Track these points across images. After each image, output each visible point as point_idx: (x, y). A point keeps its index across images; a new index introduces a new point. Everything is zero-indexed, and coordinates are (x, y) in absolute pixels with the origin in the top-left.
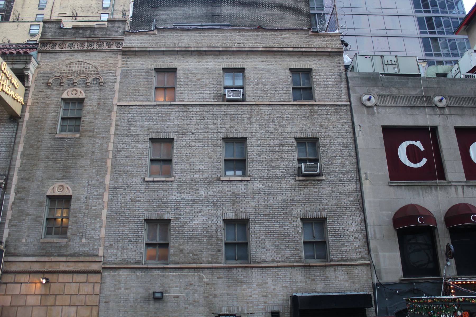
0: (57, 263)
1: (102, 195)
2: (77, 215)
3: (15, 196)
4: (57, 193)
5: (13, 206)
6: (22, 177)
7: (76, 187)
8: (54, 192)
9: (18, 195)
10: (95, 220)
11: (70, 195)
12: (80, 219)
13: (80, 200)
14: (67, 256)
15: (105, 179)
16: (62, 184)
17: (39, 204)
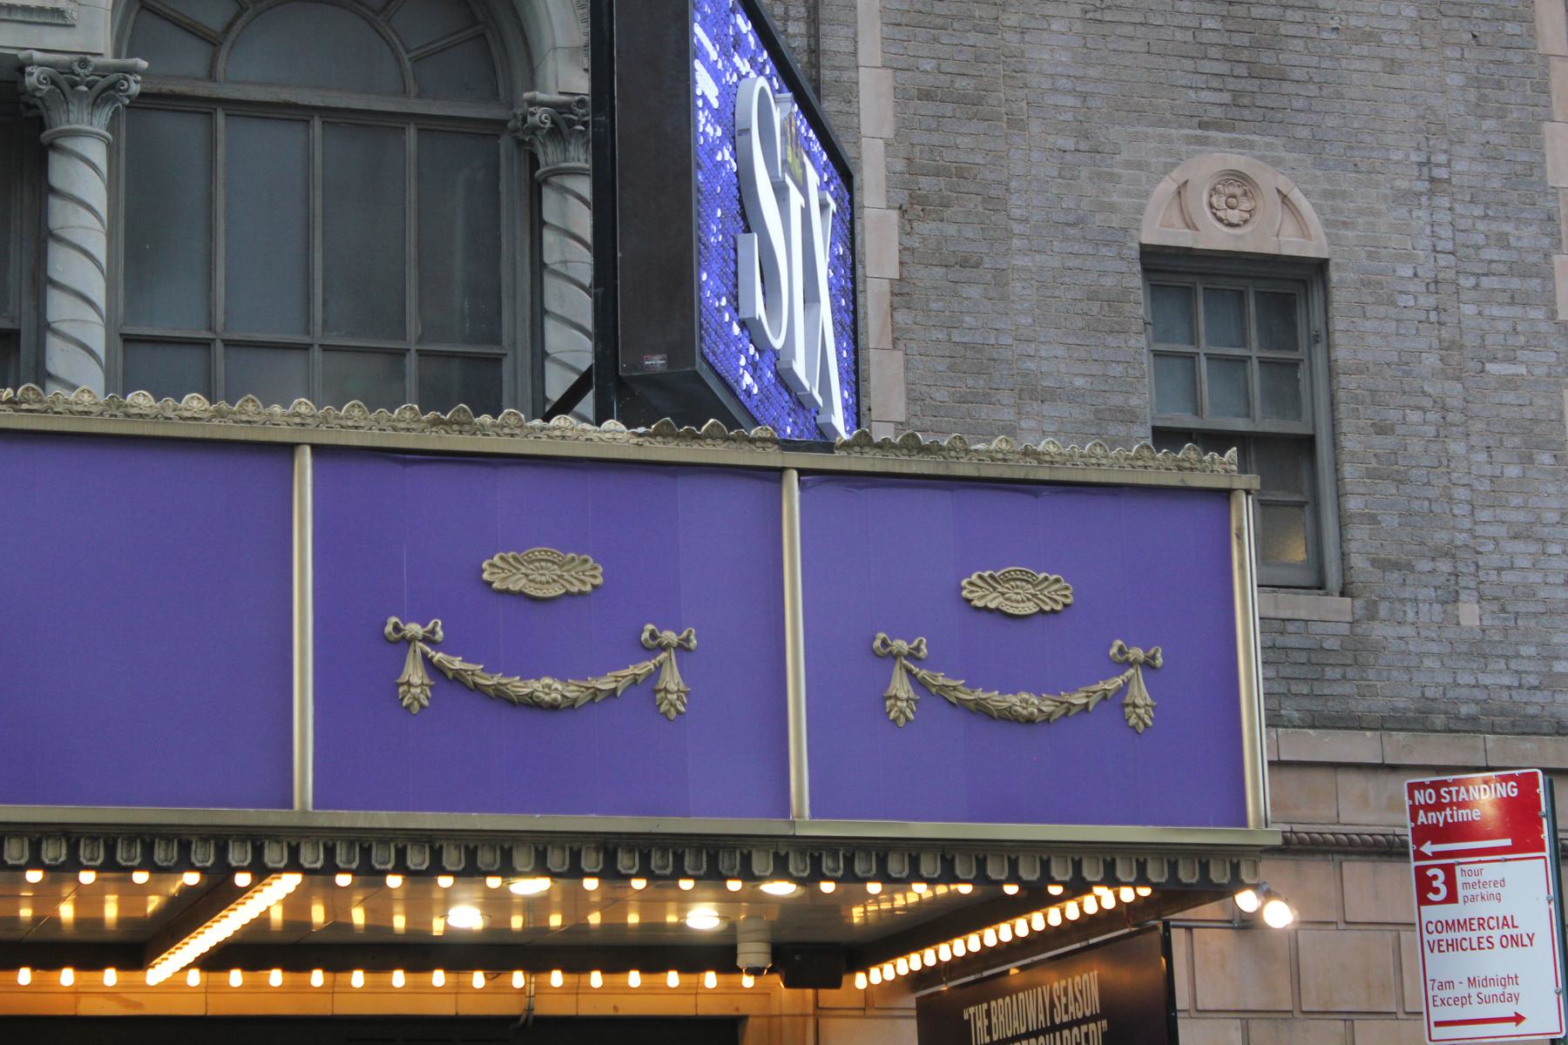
0: (1320, 778)
1: (1548, 276)
2: (1393, 415)
3: (906, 231)
4: (1214, 237)
5: (899, 316)
6: (928, 82)
7: (1343, 195)
8: (1191, 225)
9: (925, 228)
10: (1530, 459)
11: (1311, 253)
12: (1416, 446)
13: (1393, 303)
14: (1384, 724)
15: (1540, 149)
16: (1236, 161)
17: (1095, 308)
